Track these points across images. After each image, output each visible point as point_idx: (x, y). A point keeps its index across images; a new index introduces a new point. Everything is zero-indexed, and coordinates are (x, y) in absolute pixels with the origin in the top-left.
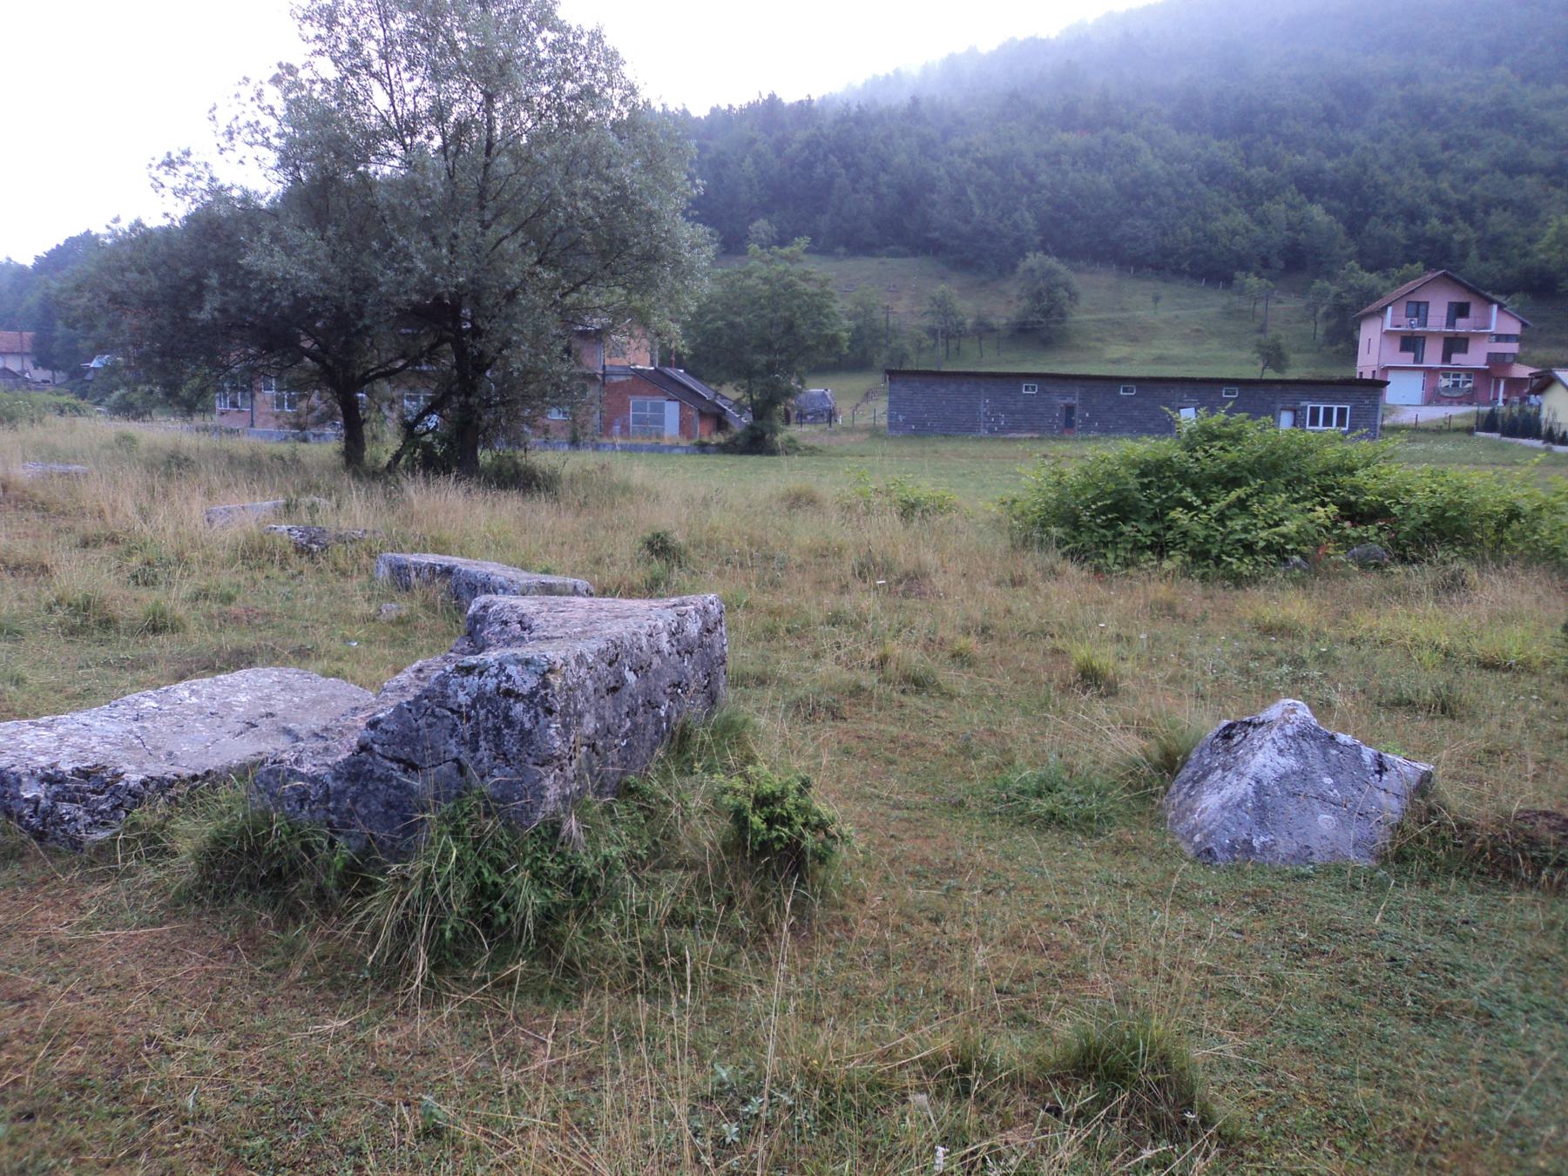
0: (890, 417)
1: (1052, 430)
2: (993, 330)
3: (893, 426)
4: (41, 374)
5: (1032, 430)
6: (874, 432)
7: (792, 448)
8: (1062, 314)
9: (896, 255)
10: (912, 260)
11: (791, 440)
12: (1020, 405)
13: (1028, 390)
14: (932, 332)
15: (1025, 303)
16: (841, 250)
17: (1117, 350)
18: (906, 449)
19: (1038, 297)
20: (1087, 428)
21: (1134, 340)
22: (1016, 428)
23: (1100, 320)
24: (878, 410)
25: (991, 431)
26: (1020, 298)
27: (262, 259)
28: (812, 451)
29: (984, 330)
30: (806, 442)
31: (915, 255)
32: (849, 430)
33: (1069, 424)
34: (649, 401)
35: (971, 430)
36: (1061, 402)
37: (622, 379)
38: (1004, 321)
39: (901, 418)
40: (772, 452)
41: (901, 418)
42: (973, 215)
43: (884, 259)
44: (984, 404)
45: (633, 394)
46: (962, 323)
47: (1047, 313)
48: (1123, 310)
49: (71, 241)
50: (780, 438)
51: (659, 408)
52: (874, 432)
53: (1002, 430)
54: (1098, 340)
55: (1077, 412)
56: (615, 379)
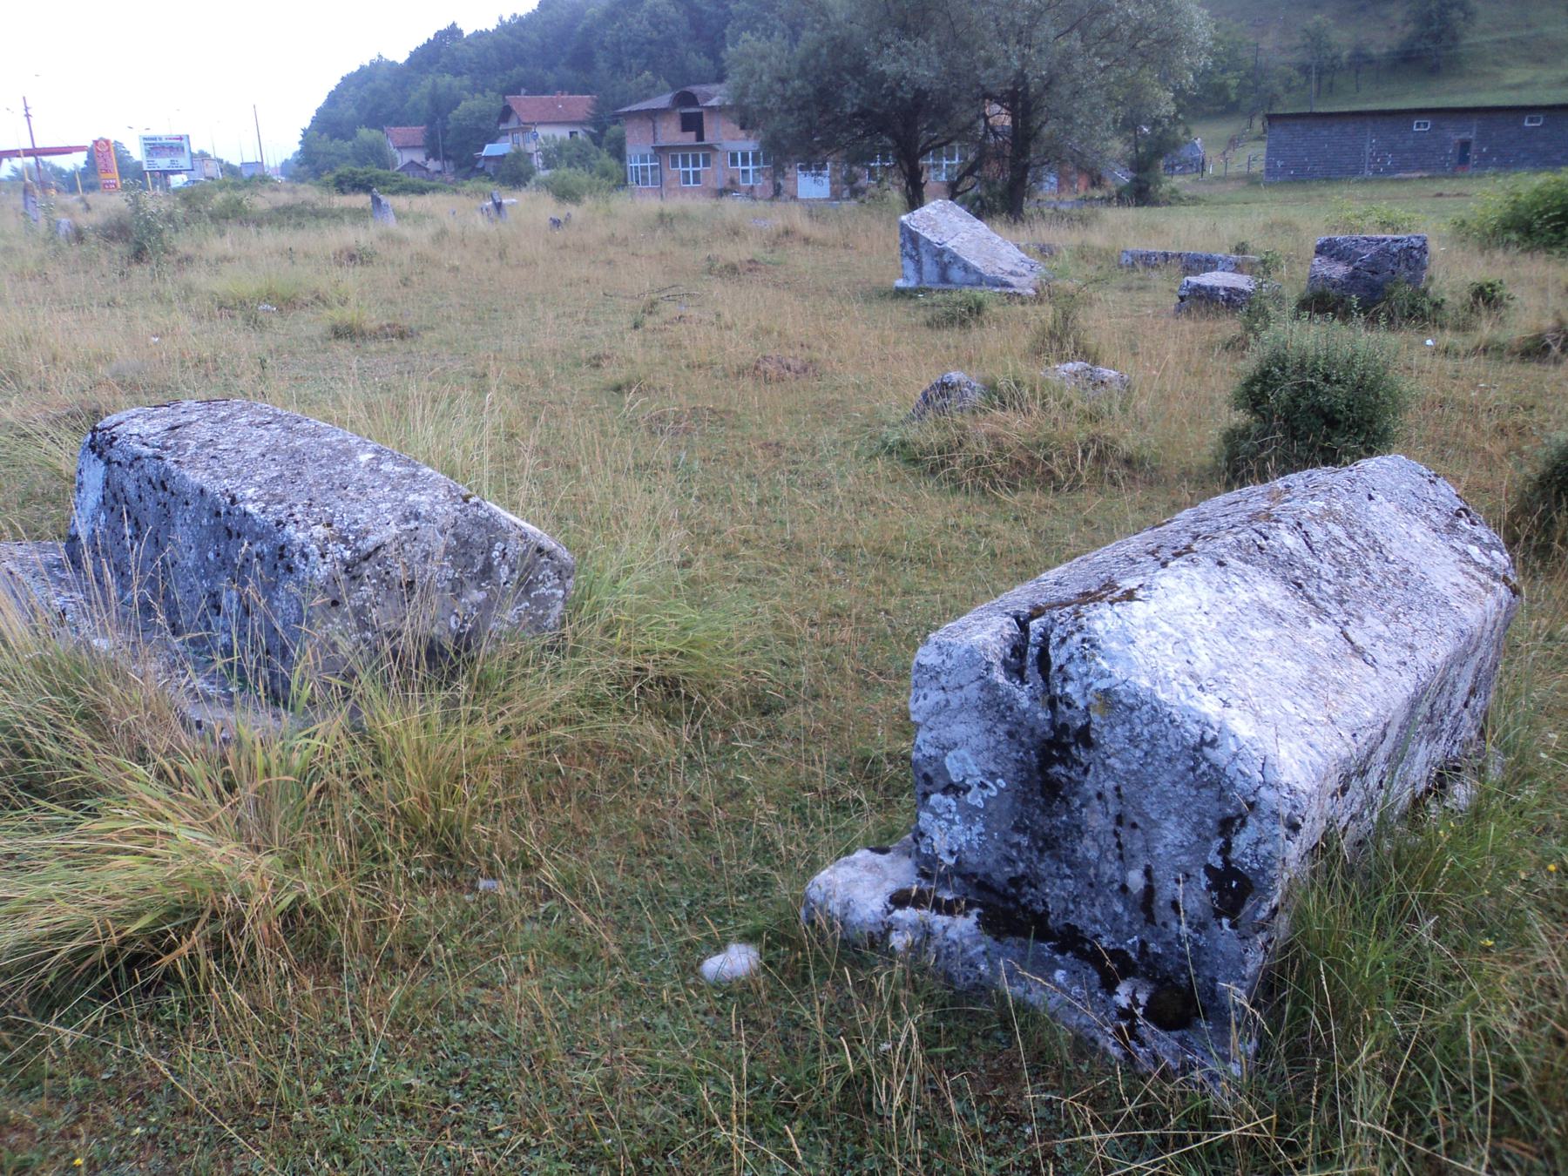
0: (1268, 164)
1: (1445, 168)
2: (1371, 62)
3: (1270, 171)
4: (433, 165)
5: (1422, 168)
6: (1251, 180)
7: (1175, 199)
8: (1454, 38)
11: (1174, 191)
12: (1410, 143)
13: (1419, 127)
14: (1304, 69)
15: (1411, 28)
17: (1518, 74)
18: (1291, 195)
19: (1427, 20)
20: (1484, 162)
21: (1541, 61)
22: (1403, 166)
23: (1500, 42)
24: (1252, 157)
25: (1376, 171)
26: (1406, 23)
28: (1195, 200)
29: (1361, 61)
30: (1188, 192)
32: (1224, 179)
33: (1463, 160)
35: (1355, 172)
36: (1457, 138)
38: (1385, 50)
39: (1279, 163)
40: (1155, 203)
41: (1279, 163)
44: (1370, 142)
46: (1336, 57)
47: (1437, 38)
48: (1529, 26)
49: (439, 35)
50: (1164, 188)
52: (1251, 180)
53: (1388, 171)
54: (1496, 63)
55: (1473, 147)
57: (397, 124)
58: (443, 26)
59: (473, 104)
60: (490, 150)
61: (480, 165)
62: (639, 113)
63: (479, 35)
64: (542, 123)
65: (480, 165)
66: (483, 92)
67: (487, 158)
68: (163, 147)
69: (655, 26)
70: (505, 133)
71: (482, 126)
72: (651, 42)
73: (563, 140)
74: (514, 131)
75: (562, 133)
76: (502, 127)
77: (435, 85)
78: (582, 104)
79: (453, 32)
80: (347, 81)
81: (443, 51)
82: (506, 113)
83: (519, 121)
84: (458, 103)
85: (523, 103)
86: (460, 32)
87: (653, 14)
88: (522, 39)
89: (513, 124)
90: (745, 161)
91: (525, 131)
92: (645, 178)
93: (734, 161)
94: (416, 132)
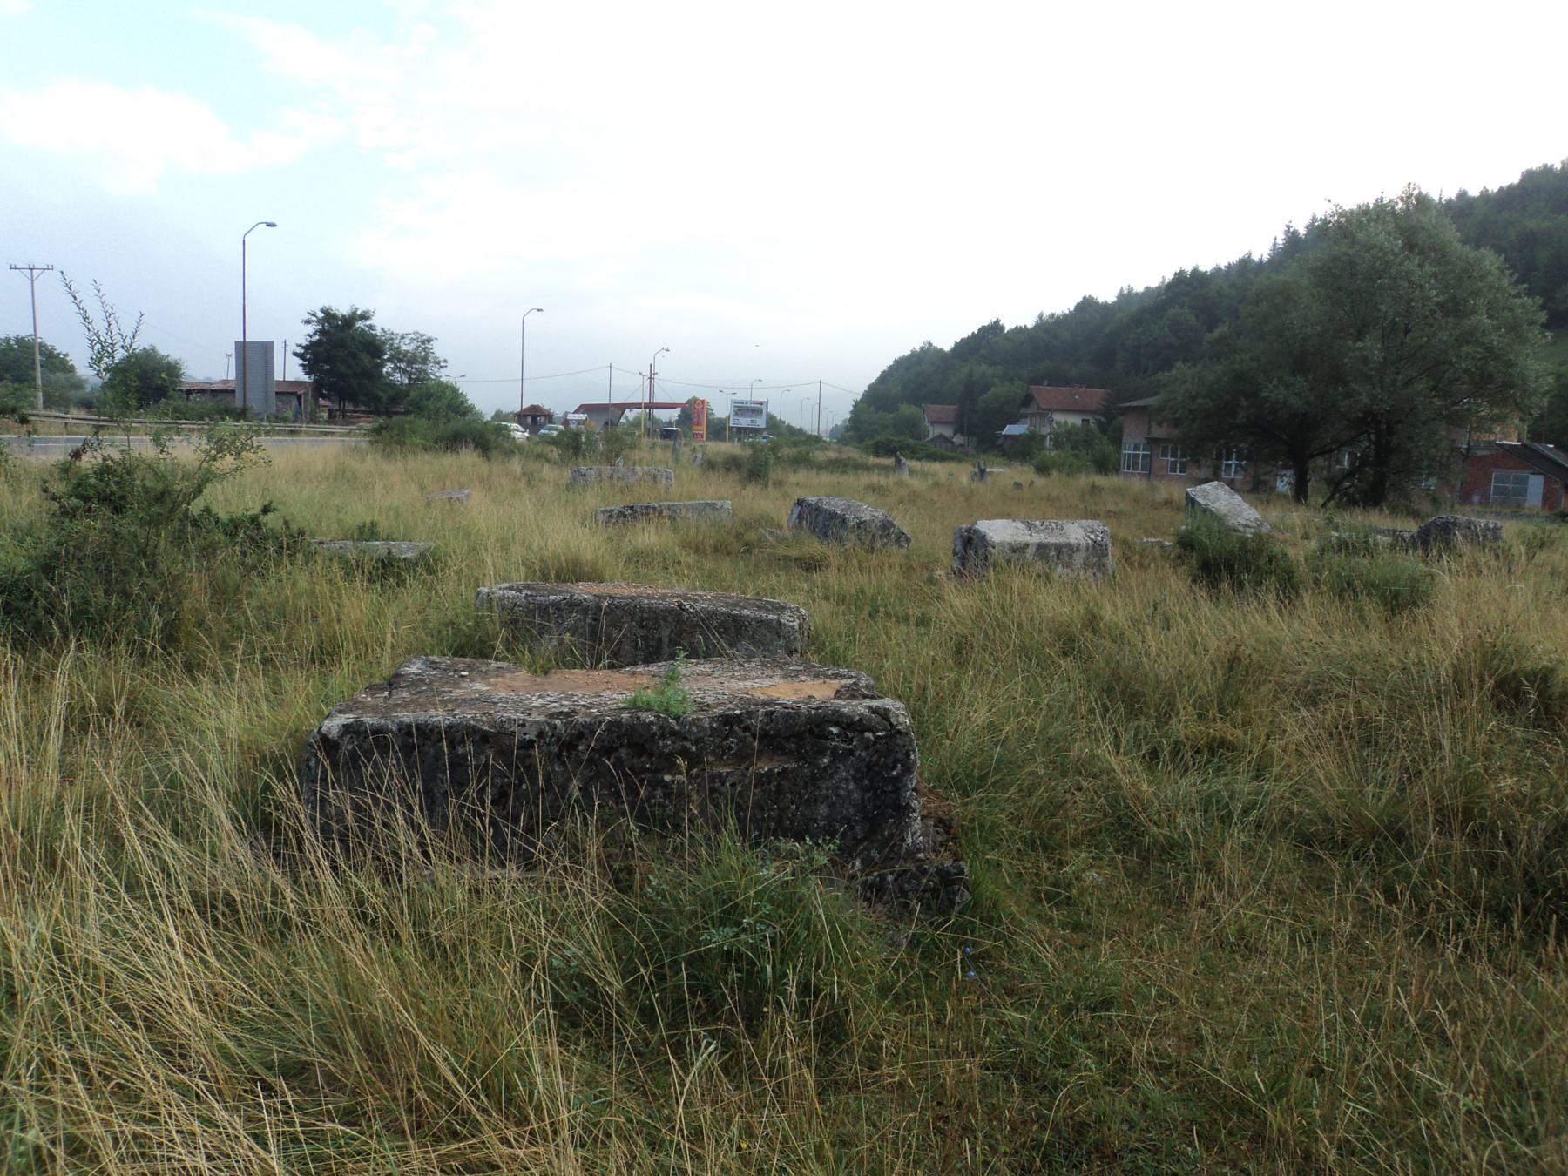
4: (958, 439)
27: (1273, 392)
34: (1513, 474)
37: (1484, 453)
49: (983, 330)
51: (1525, 481)
56: (1479, 453)
57: (935, 402)
59: (1001, 390)
60: (1010, 430)
61: (999, 442)
62: (1143, 410)
64: (1057, 411)
65: (999, 442)
66: (1011, 381)
67: (1007, 437)
68: (747, 409)
70: (1024, 416)
73: (1073, 426)
74: (1033, 415)
75: (1075, 420)
76: (1023, 411)
77: (971, 375)
78: (1096, 396)
80: (898, 363)
81: (988, 343)
82: (1028, 400)
85: (1045, 394)
86: (1002, 328)
89: (1032, 409)
91: (1042, 416)
92: (1136, 463)
94: (949, 410)
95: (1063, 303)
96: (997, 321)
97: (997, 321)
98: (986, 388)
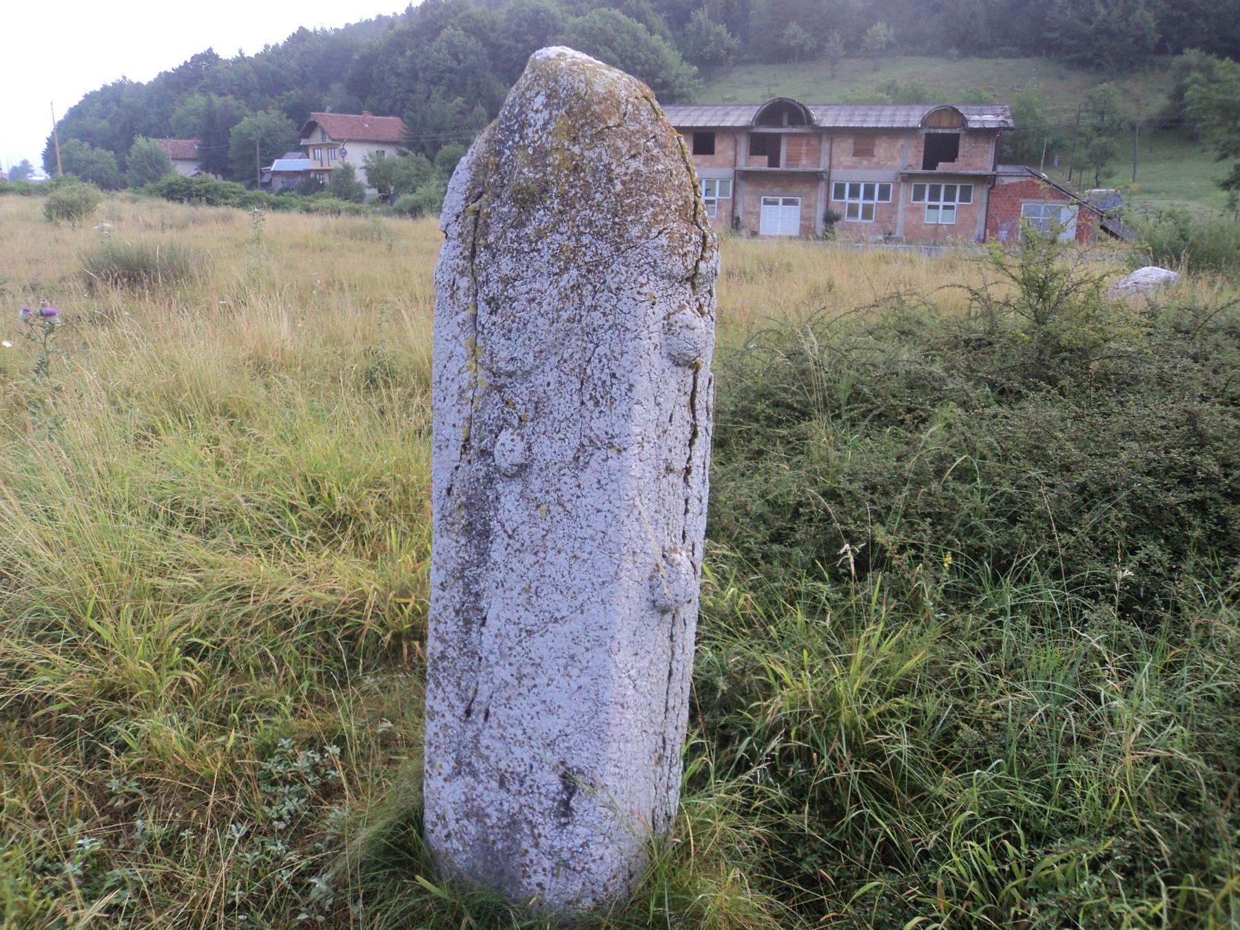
9: (1009, 56)
10: (1027, 61)
16: (953, 51)
31: (1029, 56)
37: (1014, 180)
42: (1096, 14)
43: (1002, 60)
45: (1029, 196)
49: (197, 58)
56: (1007, 181)
58: (201, 50)
59: (256, 122)
60: (278, 165)
63: (241, 60)
64: (349, 141)
65: (266, 179)
66: (265, 108)
67: (276, 173)
69: (455, 56)
71: (267, 140)
72: (451, 70)
76: (303, 142)
78: (392, 126)
79: (209, 57)
80: (90, 98)
81: (200, 73)
83: (323, 132)
84: (241, 120)
87: (451, 44)
88: (281, 66)
89: (316, 138)
90: (854, 192)
91: (330, 147)
93: (839, 193)
94: (194, 145)
95: (279, 36)
96: (210, 49)
97: (210, 49)
98: (235, 120)
